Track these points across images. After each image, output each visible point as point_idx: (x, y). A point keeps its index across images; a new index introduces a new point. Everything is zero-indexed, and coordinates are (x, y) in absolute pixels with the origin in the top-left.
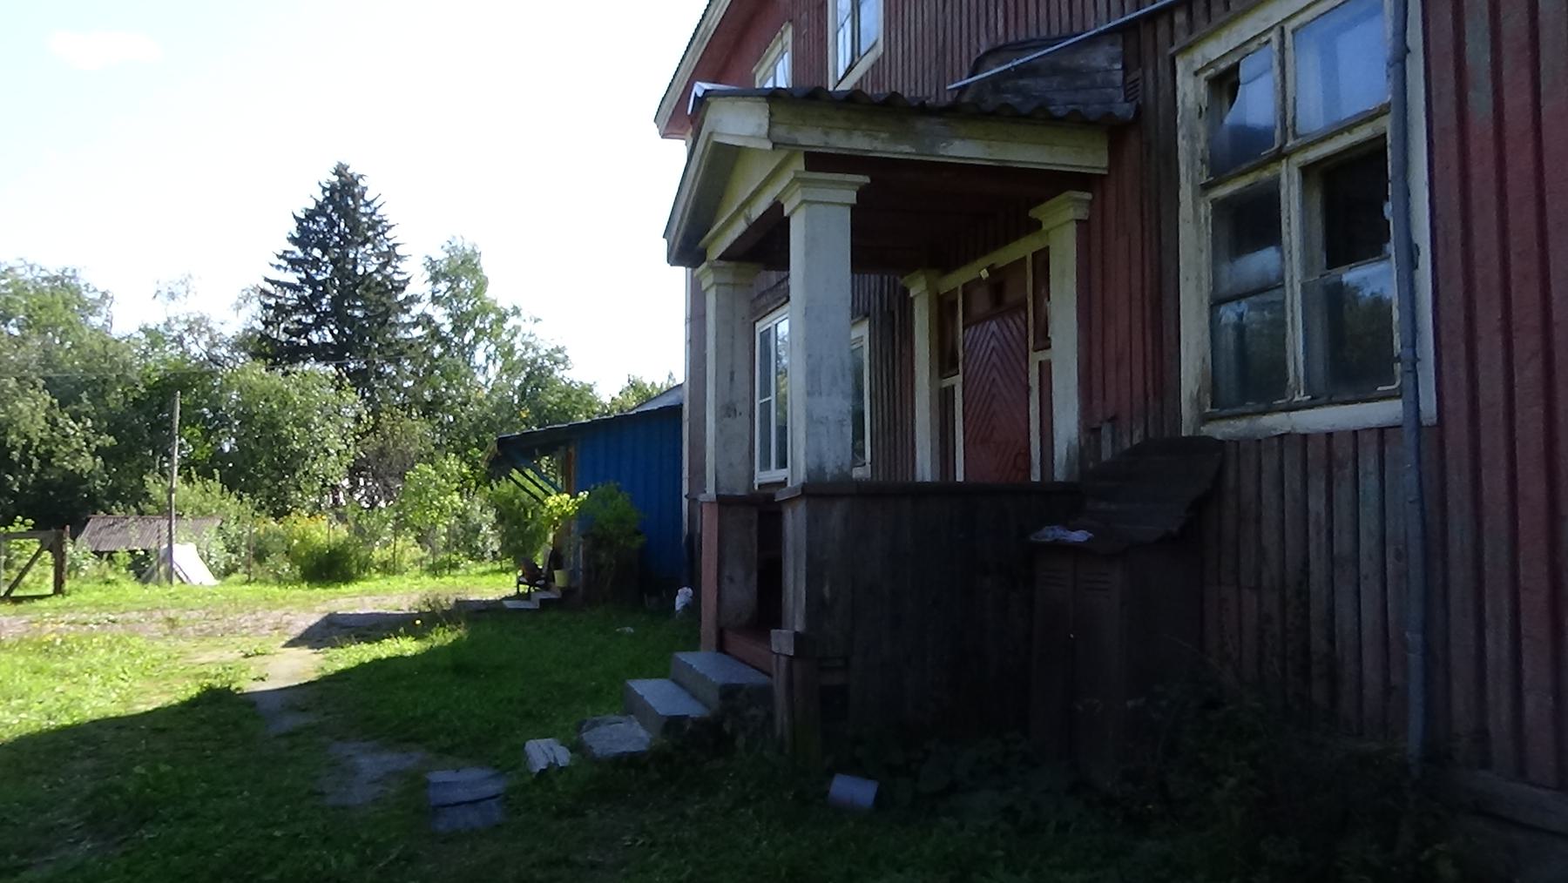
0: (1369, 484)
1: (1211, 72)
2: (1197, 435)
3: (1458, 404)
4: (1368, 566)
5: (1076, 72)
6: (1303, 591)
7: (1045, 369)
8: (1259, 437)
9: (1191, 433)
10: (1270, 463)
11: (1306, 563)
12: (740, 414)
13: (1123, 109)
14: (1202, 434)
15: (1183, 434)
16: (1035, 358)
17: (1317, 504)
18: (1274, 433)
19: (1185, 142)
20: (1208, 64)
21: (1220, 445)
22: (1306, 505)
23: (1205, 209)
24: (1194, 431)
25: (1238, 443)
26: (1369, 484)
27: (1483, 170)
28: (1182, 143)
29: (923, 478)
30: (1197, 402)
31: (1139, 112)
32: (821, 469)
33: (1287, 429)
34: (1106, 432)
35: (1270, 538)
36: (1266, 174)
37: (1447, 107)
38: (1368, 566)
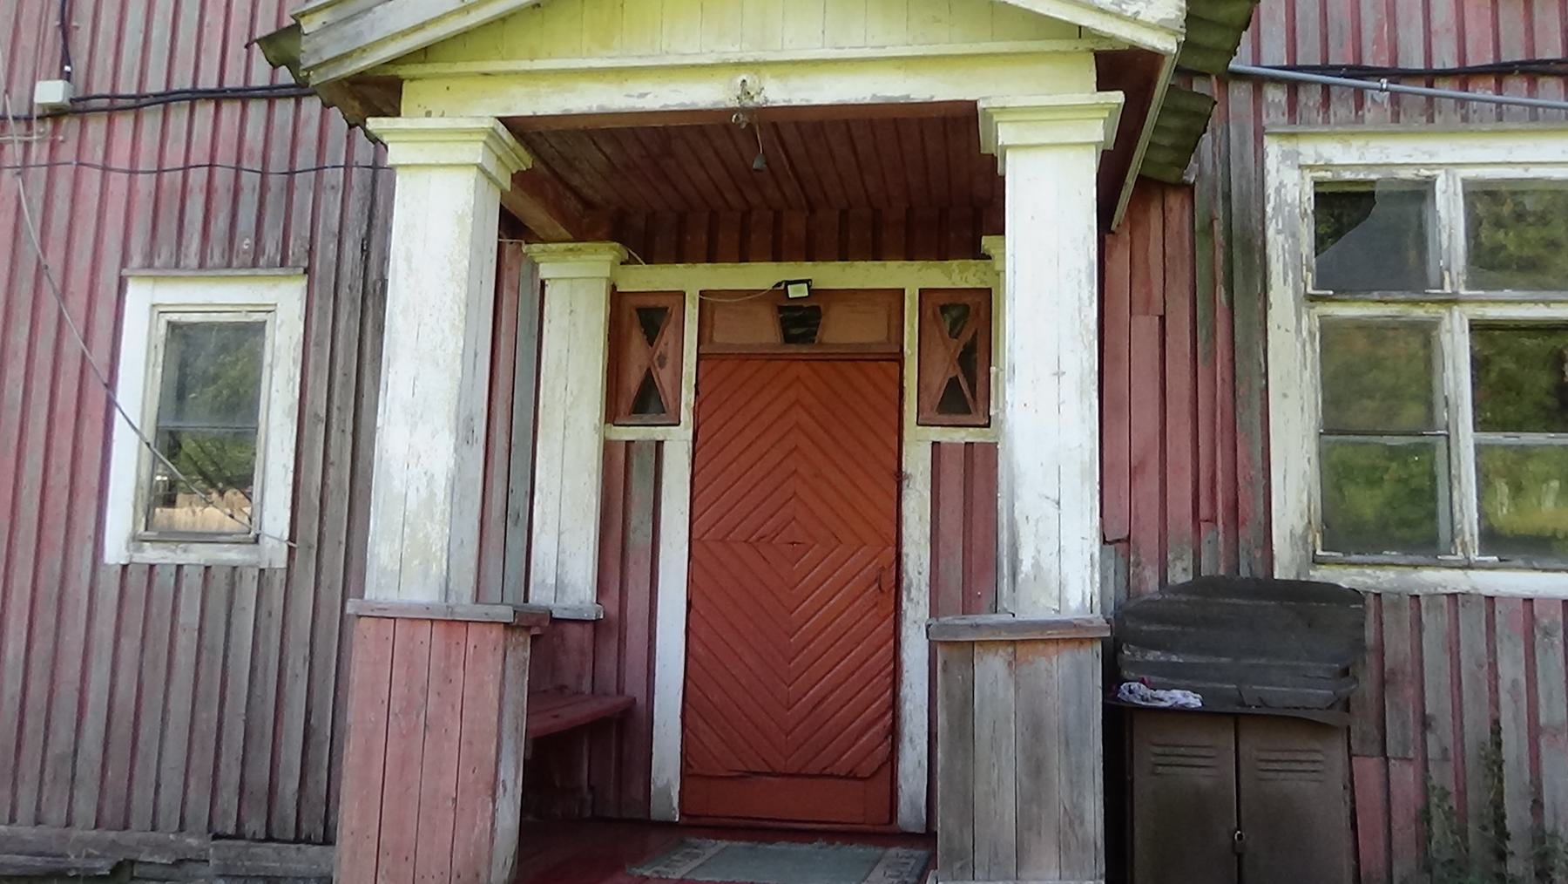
1: (1329, 175)
2: (1303, 579)
6: (1494, 765)
8: (1416, 592)
9: (1292, 577)
11: (1496, 729)
14: (1313, 580)
15: (1276, 577)
17: (1511, 669)
18: (1441, 590)
20: (1326, 165)
21: (1355, 596)
22: (1493, 666)
23: (1311, 319)
24: (1298, 574)
25: (1378, 595)
29: (559, 586)
33: (1464, 588)
35: (1437, 702)
36: (1419, 313)
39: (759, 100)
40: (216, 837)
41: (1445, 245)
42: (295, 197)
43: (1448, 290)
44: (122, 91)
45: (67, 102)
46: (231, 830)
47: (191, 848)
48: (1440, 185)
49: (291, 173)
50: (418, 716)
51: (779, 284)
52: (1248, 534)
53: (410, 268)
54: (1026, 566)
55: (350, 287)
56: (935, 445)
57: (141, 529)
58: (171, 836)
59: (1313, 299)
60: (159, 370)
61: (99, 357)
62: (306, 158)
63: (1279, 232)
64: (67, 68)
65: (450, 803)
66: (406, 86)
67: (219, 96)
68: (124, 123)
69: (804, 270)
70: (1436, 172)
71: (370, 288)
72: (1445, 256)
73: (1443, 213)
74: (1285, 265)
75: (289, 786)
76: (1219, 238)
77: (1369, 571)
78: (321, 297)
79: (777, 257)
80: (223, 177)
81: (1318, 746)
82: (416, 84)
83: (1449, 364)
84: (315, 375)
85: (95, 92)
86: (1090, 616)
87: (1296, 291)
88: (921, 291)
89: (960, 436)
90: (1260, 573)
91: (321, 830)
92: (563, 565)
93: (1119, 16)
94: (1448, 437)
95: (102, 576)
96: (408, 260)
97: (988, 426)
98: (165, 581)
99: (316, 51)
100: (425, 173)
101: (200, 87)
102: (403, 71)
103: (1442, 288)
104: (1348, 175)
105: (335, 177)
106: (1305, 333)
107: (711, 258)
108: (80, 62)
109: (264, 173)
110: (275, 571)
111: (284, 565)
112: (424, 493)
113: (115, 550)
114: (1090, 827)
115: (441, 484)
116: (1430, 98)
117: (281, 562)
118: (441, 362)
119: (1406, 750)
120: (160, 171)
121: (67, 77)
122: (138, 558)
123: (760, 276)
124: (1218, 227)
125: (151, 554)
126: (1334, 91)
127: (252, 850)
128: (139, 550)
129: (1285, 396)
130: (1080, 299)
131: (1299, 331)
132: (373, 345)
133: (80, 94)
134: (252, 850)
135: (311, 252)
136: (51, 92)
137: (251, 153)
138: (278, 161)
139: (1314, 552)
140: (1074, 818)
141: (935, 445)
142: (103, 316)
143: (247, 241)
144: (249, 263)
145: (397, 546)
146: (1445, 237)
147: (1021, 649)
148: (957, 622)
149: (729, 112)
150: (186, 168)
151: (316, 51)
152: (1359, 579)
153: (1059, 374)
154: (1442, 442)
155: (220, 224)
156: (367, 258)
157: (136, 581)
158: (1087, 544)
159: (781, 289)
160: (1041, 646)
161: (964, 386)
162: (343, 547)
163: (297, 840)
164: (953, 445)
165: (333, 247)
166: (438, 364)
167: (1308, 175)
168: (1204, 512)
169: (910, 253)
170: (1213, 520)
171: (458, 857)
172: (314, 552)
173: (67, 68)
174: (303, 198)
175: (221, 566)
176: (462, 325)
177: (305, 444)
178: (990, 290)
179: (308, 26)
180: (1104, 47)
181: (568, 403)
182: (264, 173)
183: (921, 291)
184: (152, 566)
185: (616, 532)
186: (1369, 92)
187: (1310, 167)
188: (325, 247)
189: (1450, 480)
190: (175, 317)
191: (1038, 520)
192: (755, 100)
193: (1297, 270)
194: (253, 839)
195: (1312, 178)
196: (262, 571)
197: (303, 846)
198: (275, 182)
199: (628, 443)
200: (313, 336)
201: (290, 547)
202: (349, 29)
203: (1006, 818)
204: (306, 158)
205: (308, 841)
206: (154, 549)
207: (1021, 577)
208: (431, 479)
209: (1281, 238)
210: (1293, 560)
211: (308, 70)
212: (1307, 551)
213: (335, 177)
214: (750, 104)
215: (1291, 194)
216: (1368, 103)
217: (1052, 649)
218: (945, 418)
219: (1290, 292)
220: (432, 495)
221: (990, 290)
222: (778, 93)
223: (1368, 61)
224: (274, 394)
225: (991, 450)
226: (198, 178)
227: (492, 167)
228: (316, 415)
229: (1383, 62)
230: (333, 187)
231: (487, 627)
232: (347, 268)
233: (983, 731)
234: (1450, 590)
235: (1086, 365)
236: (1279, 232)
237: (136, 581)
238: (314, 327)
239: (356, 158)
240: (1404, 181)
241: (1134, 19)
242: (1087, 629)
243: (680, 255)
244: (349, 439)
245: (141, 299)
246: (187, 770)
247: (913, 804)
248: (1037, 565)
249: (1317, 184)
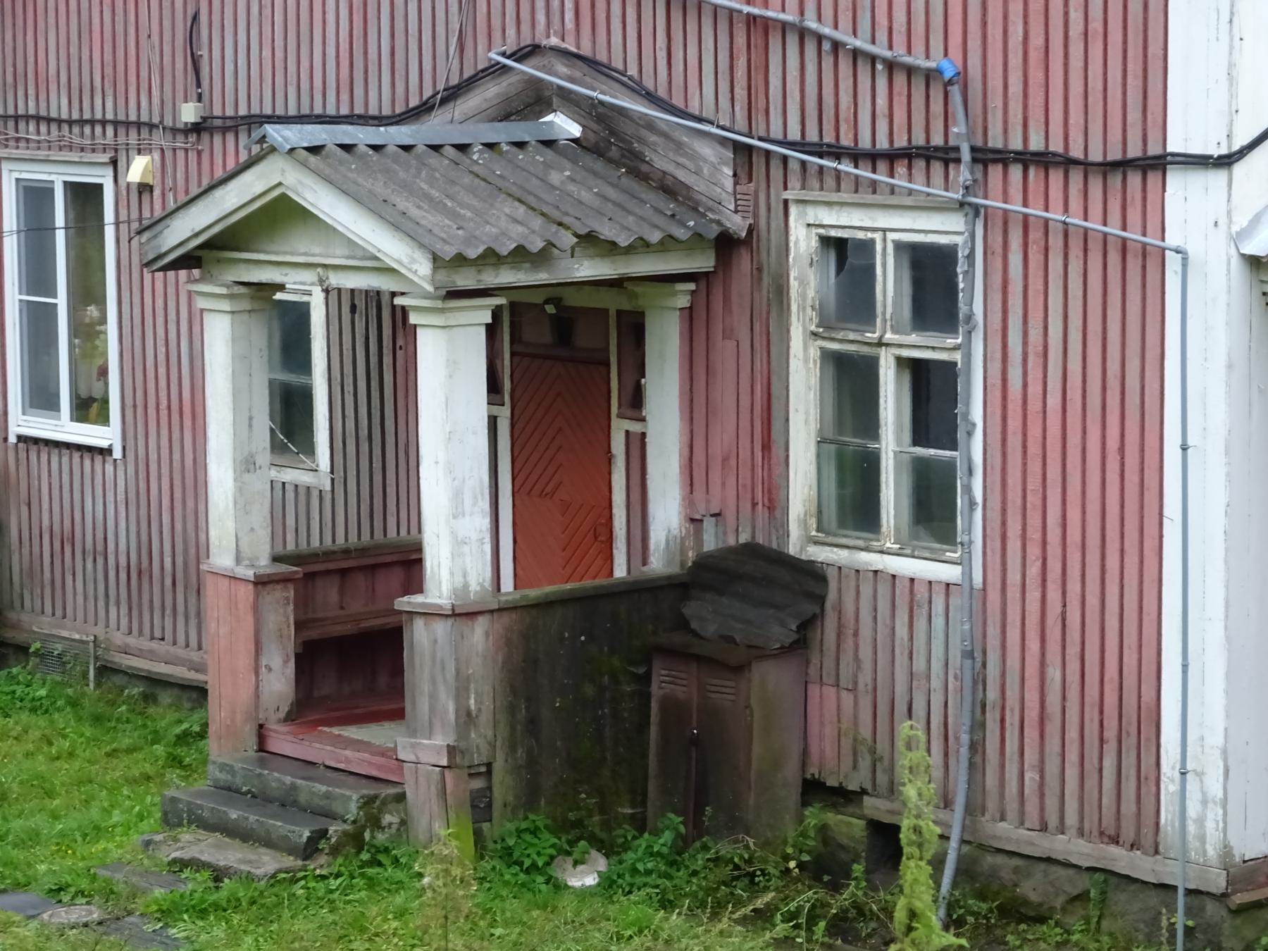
0: (938, 622)
3: (994, 578)
4: (936, 683)
5: (679, 146)
7: (638, 446)
10: (866, 591)
12: (260, 468)
13: (737, 224)
16: (619, 429)
17: (902, 631)
22: (893, 628)
23: (814, 353)
26: (938, 622)
27: (1014, 423)
28: (794, 284)
30: (804, 524)
31: (750, 230)
32: (466, 586)
33: (879, 567)
34: (709, 524)
35: (865, 653)
37: (996, 379)
38: (936, 683)
45: (199, 120)
77: (835, 549)
115: (231, 499)
136: (189, 113)
152: (831, 555)
153: (437, 463)
167: (814, 231)
195: (817, 234)
215: (803, 245)
248: (432, 571)
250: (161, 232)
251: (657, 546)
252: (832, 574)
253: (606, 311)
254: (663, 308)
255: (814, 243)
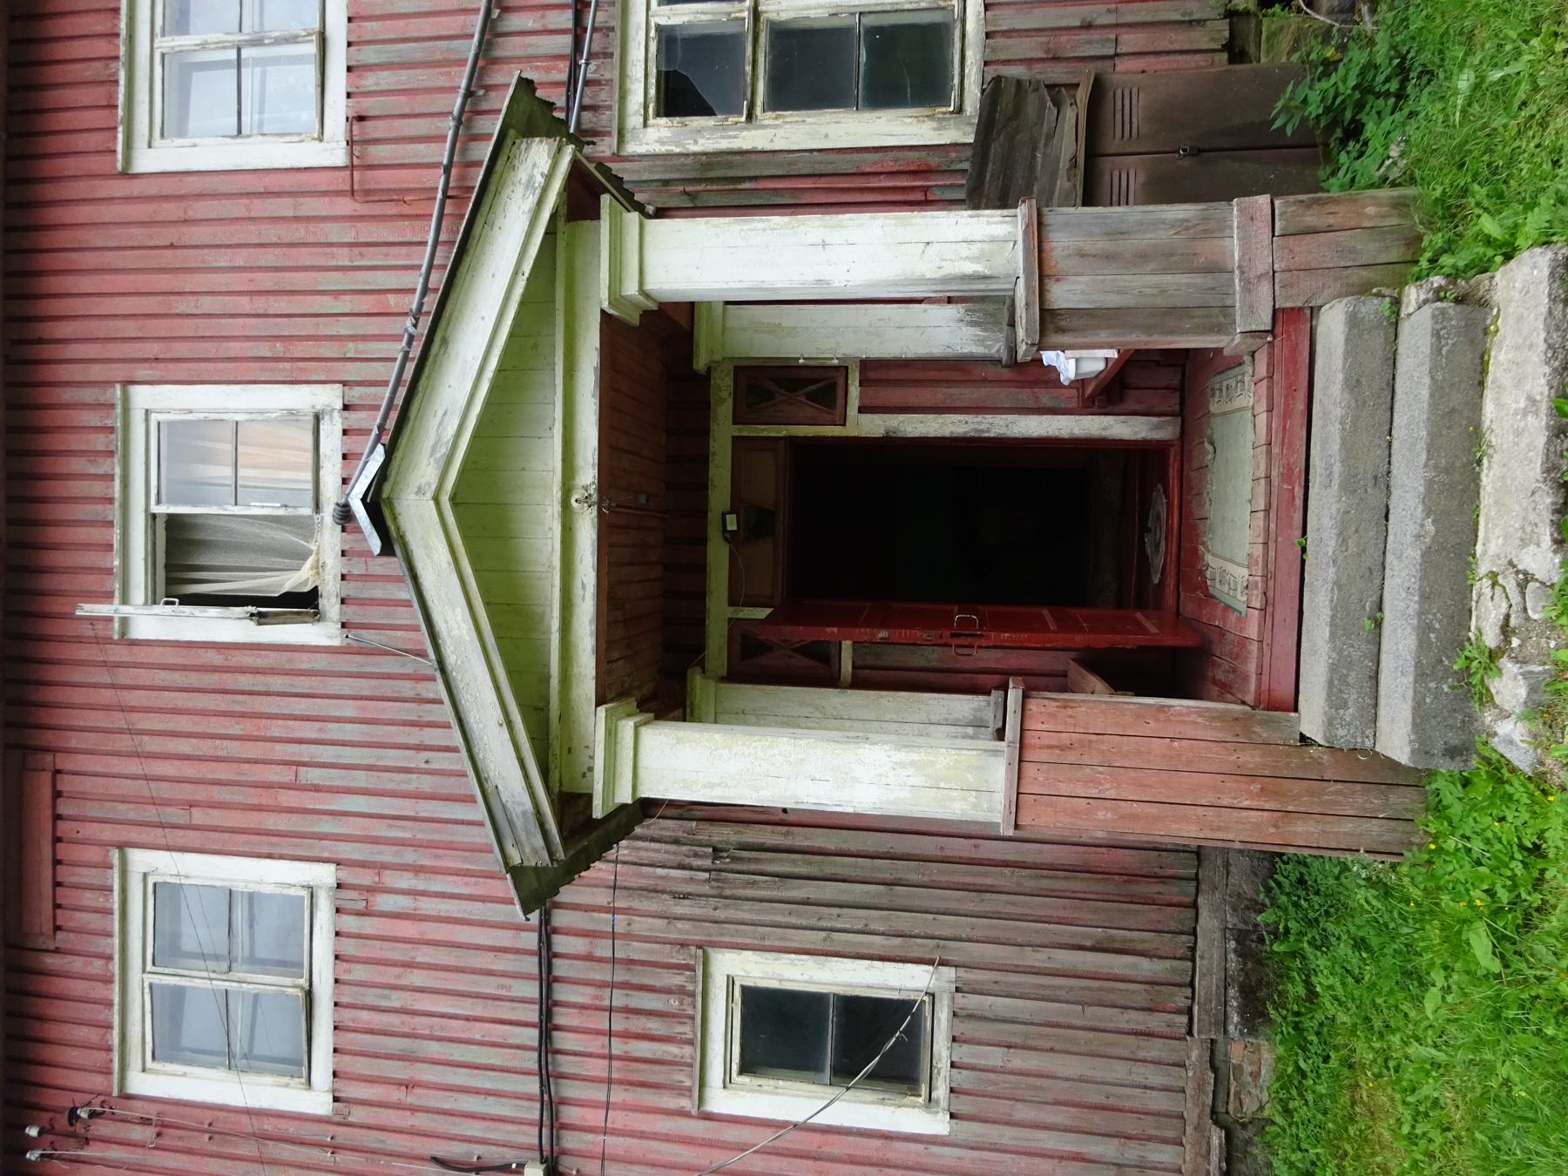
19: (701, 141)
24: (969, 124)
30: (942, 123)
39: (592, 490)
40: (1190, 1033)
41: (709, 17)
42: (636, 958)
43: (745, 14)
44: (536, 1116)
45: (544, 1166)
46: (1184, 1019)
47: (1201, 1056)
48: (663, 21)
49: (614, 960)
50: (1100, 773)
51: (726, 539)
52: (934, 161)
53: (720, 785)
54: (979, 268)
55: (715, 909)
56: (862, 410)
57: (921, 1100)
58: (1190, 1074)
59: (750, 117)
60: (781, 1082)
61: (765, 1138)
62: (603, 949)
63: (696, 142)
64: (514, 1166)
65: (1176, 744)
66: (565, 789)
67: (547, 1027)
68: (569, 1114)
69: (713, 517)
70: (653, 25)
71: (713, 892)
72: (718, 17)
73: (685, 19)
74: (723, 137)
75: (1145, 967)
76: (701, 187)
78: (722, 935)
79: (703, 541)
80: (619, 1024)
81: (1111, 94)
82: (565, 781)
83: (805, 13)
84: (790, 940)
85: (536, 1141)
86: (1020, 218)
87: (744, 129)
88: (735, 423)
89: (854, 391)
90: (969, 153)
91: (1184, 938)
92: (957, 720)
93: (545, 190)
94: (861, 13)
95: (961, 1137)
96: (712, 786)
97: (847, 368)
98: (964, 1078)
99: (535, 851)
100: (642, 773)
101: (536, 1044)
102: (556, 790)
103: (744, 19)
104: (652, 92)
105: (621, 923)
106: (777, 122)
107: (700, 595)
108: (510, 1156)
109: (613, 986)
110: (958, 979)
111: (953, 969)
112: (911, 771)
113: (938, 1124)
114: (1189, 215)
115: (901, 756)
116: (594, 29)
117: (949, 973)
118: (800, 757)
119: (1108, 40)
120: (610, 1081)
121: (521, 1166)
122: (944, 1104)
123: (718, 555)
124: (690, 188)
125: (941, 1092)
126: (587, 101)
127: (1202, 1001)
128: (937, 1102)
129: (826, 136)
130: (764, 230)
131: (777, 126)
132: (764, 889)
133: (538, 1155)
134: (1202, 1001)
135: (684, 945)
137: (596, 997)
138: (602, 973)
139: (951, 113)
140: (1183, 225)
141: (862, 410)
142: (731, 1134)
143: (672, 1001)
144: (689, 1000)
145: (954, 794)
146: (703, 17)
147: (1048, 271)
148: (1024, 321)
149: (600, 514)
150: (611, 1057)
151: (535, 851)
153: (824, 245)
154: (867, 21)
155: (654, 1026)
156: (690, 894)
157: (964, 1105)
158: (962, 221)
159: (730, 537)
160: (1044, 255)
161: (813, 387)
162: (938, 917)
163: (1193, 960)
164: (861, 397)
165: (679, 925)
166: (802, 760)
167: (651, 121)
168: (919, 196)
169: (704, 433)
170: (925, 189)
171: (1220, 736)
172: (942, 942)
173: (514, 1166)
174: (637, 951)
175: (952, 1027)
176: (769, 739)
177: (848, 950)
178: (737, 369)
179: (516, 859)
180: (563, 211)
181: (820, 716)
182: (613, 986)
183: (735, 423)
184: (952, 1090)
185: (932, 677)
186: (588, 75)
187: (646, 119)
188: (680, 931)
189: (896, 11)
190: (735, 1068)
191: (943, 260)
192: (592, 491)
193: (724, 128)
194: (1193, 998)
196: (958, 990)
197: (1198, 953)
198: (621, 976)
199: (854, 667)
200: (756, 942)
201: (940, 964)
202: (519, 823)
203: (1184, 281)
204: (603, 949)
205: (1193, 949)
206: (937, 1089)
207: (988, 272)
208: (902, 765)
209: (701, 141)
210: (958, 128)
211: (552, 860)
212: (949, 119)
213: (621, 923)
214: (595, 498)
216: (596, 76)
217: (1046, 246)
218: (840, 401)
219: (745, 133)
220: (913, 764)
221: (737, 369)
222: (588, 475)
223: (564, 76)
224: (806, 977)
225: (867, 365)
226: (618, 1047)
227: (637, 719)
228: (825, 939)
229: (564, 66)
230: (629, 924)
231: (1028, 713)
232: (698, 911)
233: (1113, 301)
234: (982, 9)
235: (817, 224)
236: (696, 142)
237: (964, 1105)
238: (747, 941)
239: (605, 904)
240: (658, 51)
241: (549, 177)
242: (1030, 217)
243: (698, 622)
244: (846, 911)
245: (721, 1101)
246: (1131, 1060)
247: (1157, 427)
249: (658, 114)
250: (504, 807)
251: (981, 341)
252: (992, 72)
253: (734, 438)
254: (724, 329)
255: (663, 121)
